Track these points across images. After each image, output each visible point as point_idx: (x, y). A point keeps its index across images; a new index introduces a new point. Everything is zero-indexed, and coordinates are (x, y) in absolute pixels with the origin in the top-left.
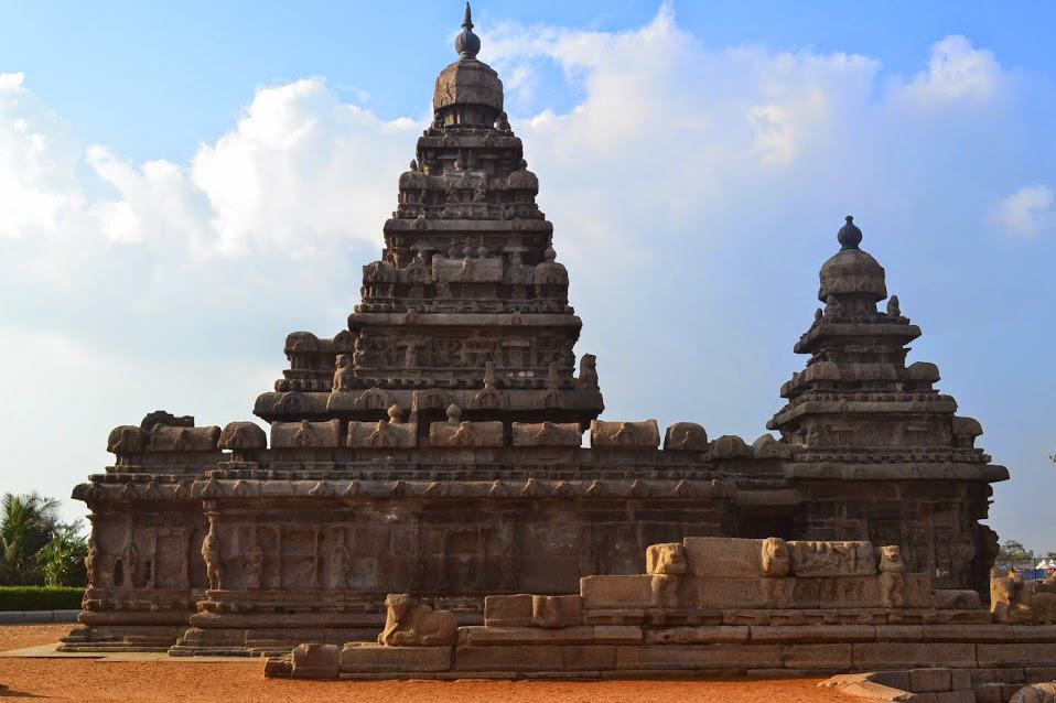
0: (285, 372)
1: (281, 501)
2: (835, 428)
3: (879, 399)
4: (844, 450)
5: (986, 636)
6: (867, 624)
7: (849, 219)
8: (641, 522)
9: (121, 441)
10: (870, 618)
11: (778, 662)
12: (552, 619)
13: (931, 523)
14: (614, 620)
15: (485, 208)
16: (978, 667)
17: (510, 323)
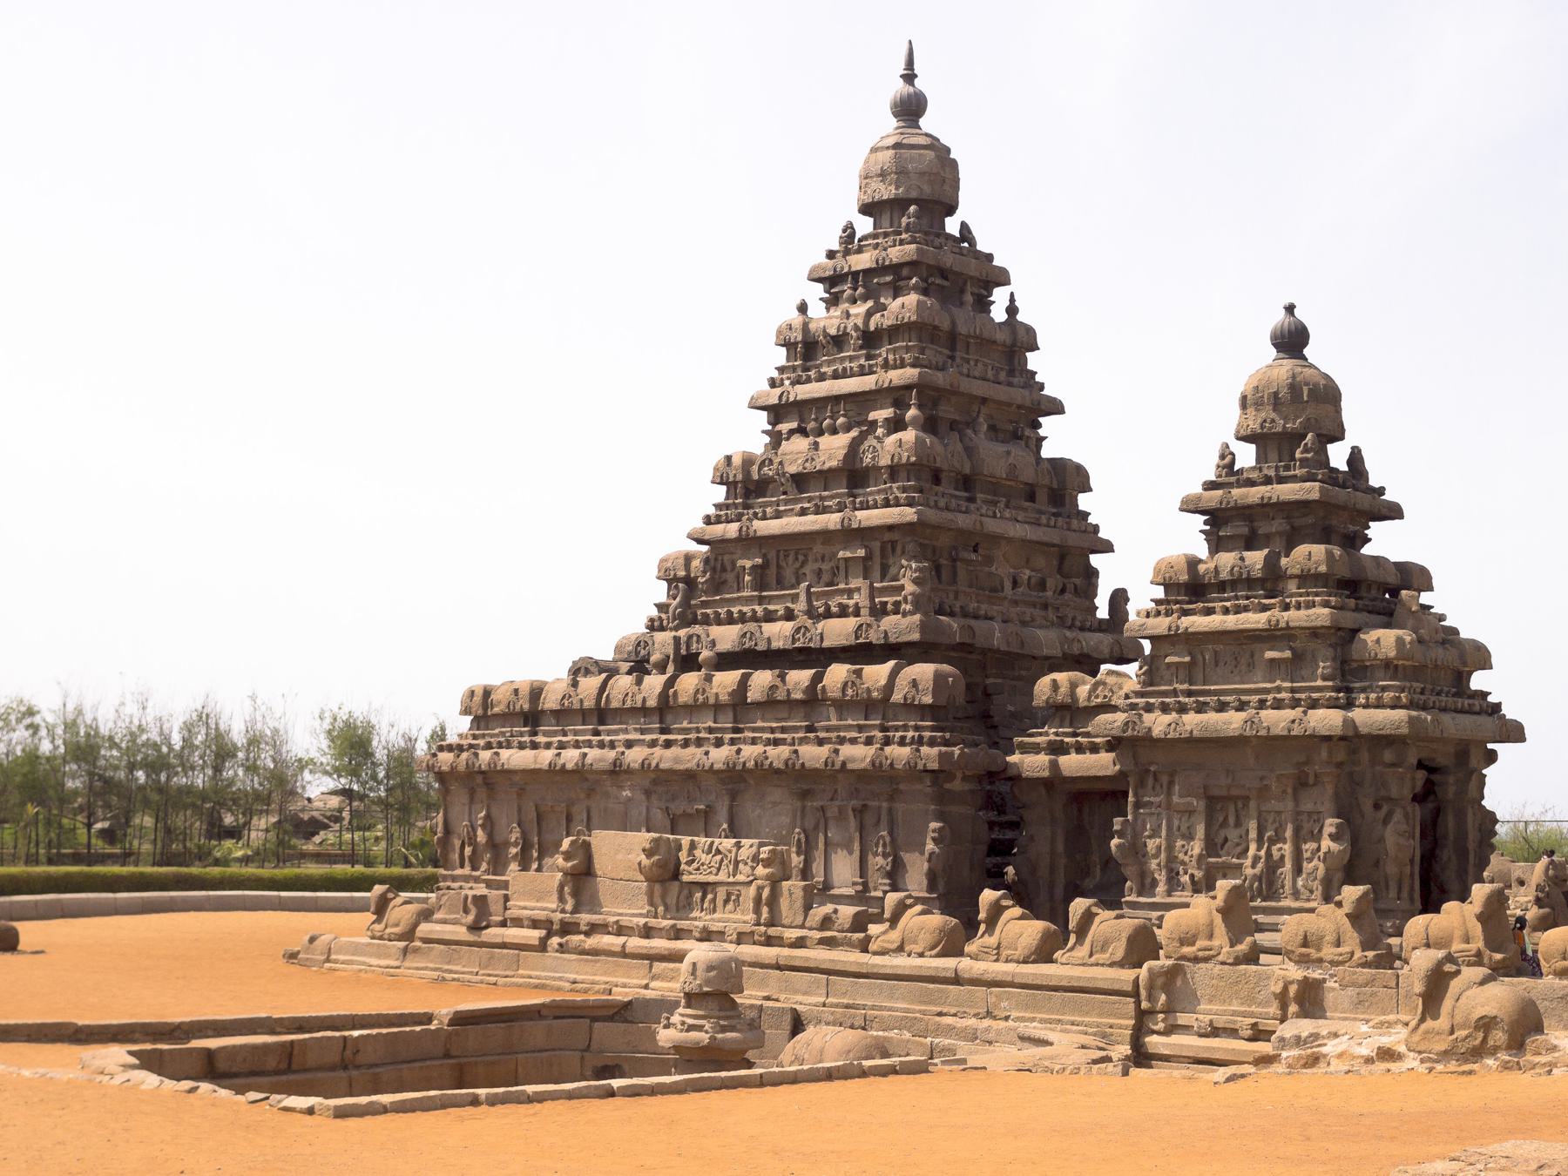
0: (656, 605)
1: (533, 773)
2: (1168, 660)
3: (1226, 611)
4: (1175, 693)
5: (838, 968)
6: (731, 942)
7: (1290, 309)
8: (854, 802)
10: (735, 936)
11: (645, 982)
12: (470, 918)
13: (1290, 805)
14: (526, 923)
15: (862, 361)
16: (824, 1005)
17: (839, 527)
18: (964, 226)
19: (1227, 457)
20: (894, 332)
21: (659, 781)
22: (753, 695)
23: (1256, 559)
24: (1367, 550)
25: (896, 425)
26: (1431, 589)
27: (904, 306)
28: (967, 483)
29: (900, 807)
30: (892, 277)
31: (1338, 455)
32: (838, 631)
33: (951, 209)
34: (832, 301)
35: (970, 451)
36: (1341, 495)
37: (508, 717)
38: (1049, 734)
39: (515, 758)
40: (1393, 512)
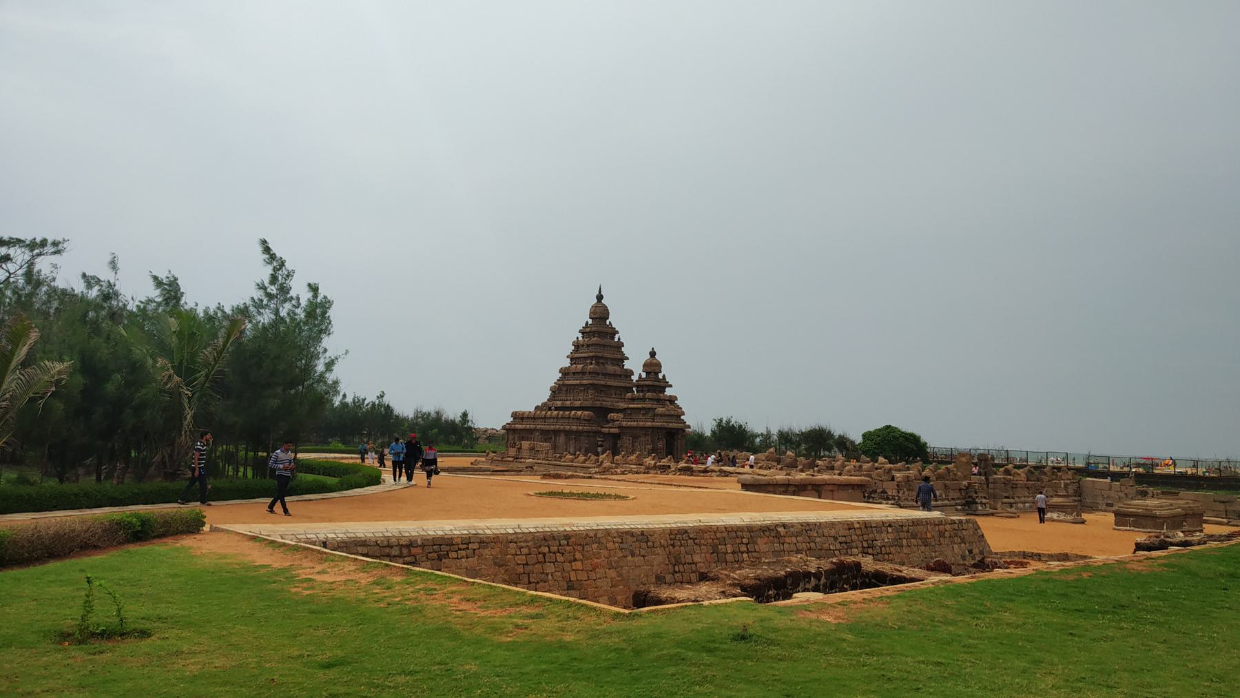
7: (653, 349)
9: (515, 415)
18: (610, 322)
19: (640, 375)
20: (592, 345)
21: (543, 432)
22: (560, 416)
23: (641, 394)
24: (665, 393)
25: (591, 364)
26: (677, 400)
27: (594, 340)
28: (603, 374)
29: (581, 438)
30: (593, 334)
31: (660, 376)
32: (577, 403)
33: (608, 319)
34: (583, 337)
35: (606, 369)
36: (657, 383)
37: (518, 418)
38: (610, 425)
39: (518, 426)
40: (671, 386)
